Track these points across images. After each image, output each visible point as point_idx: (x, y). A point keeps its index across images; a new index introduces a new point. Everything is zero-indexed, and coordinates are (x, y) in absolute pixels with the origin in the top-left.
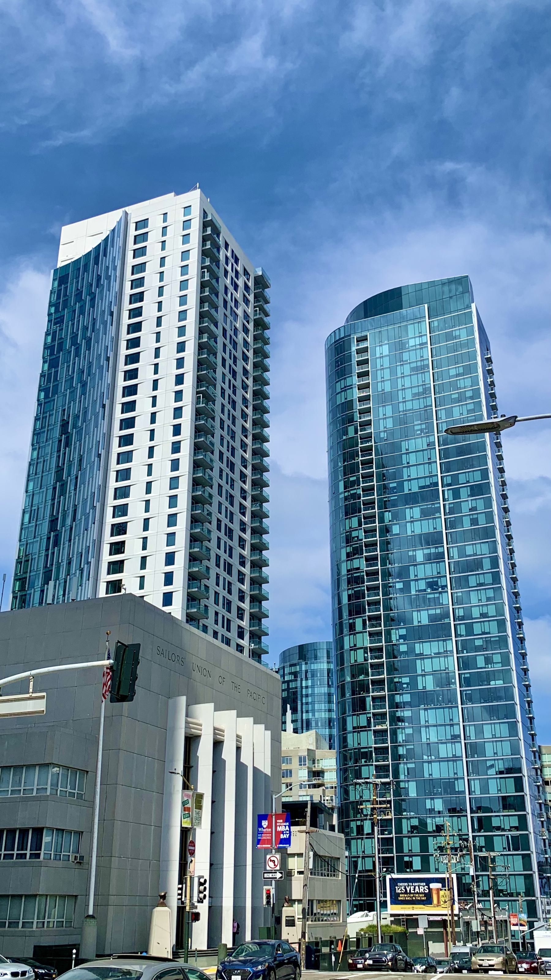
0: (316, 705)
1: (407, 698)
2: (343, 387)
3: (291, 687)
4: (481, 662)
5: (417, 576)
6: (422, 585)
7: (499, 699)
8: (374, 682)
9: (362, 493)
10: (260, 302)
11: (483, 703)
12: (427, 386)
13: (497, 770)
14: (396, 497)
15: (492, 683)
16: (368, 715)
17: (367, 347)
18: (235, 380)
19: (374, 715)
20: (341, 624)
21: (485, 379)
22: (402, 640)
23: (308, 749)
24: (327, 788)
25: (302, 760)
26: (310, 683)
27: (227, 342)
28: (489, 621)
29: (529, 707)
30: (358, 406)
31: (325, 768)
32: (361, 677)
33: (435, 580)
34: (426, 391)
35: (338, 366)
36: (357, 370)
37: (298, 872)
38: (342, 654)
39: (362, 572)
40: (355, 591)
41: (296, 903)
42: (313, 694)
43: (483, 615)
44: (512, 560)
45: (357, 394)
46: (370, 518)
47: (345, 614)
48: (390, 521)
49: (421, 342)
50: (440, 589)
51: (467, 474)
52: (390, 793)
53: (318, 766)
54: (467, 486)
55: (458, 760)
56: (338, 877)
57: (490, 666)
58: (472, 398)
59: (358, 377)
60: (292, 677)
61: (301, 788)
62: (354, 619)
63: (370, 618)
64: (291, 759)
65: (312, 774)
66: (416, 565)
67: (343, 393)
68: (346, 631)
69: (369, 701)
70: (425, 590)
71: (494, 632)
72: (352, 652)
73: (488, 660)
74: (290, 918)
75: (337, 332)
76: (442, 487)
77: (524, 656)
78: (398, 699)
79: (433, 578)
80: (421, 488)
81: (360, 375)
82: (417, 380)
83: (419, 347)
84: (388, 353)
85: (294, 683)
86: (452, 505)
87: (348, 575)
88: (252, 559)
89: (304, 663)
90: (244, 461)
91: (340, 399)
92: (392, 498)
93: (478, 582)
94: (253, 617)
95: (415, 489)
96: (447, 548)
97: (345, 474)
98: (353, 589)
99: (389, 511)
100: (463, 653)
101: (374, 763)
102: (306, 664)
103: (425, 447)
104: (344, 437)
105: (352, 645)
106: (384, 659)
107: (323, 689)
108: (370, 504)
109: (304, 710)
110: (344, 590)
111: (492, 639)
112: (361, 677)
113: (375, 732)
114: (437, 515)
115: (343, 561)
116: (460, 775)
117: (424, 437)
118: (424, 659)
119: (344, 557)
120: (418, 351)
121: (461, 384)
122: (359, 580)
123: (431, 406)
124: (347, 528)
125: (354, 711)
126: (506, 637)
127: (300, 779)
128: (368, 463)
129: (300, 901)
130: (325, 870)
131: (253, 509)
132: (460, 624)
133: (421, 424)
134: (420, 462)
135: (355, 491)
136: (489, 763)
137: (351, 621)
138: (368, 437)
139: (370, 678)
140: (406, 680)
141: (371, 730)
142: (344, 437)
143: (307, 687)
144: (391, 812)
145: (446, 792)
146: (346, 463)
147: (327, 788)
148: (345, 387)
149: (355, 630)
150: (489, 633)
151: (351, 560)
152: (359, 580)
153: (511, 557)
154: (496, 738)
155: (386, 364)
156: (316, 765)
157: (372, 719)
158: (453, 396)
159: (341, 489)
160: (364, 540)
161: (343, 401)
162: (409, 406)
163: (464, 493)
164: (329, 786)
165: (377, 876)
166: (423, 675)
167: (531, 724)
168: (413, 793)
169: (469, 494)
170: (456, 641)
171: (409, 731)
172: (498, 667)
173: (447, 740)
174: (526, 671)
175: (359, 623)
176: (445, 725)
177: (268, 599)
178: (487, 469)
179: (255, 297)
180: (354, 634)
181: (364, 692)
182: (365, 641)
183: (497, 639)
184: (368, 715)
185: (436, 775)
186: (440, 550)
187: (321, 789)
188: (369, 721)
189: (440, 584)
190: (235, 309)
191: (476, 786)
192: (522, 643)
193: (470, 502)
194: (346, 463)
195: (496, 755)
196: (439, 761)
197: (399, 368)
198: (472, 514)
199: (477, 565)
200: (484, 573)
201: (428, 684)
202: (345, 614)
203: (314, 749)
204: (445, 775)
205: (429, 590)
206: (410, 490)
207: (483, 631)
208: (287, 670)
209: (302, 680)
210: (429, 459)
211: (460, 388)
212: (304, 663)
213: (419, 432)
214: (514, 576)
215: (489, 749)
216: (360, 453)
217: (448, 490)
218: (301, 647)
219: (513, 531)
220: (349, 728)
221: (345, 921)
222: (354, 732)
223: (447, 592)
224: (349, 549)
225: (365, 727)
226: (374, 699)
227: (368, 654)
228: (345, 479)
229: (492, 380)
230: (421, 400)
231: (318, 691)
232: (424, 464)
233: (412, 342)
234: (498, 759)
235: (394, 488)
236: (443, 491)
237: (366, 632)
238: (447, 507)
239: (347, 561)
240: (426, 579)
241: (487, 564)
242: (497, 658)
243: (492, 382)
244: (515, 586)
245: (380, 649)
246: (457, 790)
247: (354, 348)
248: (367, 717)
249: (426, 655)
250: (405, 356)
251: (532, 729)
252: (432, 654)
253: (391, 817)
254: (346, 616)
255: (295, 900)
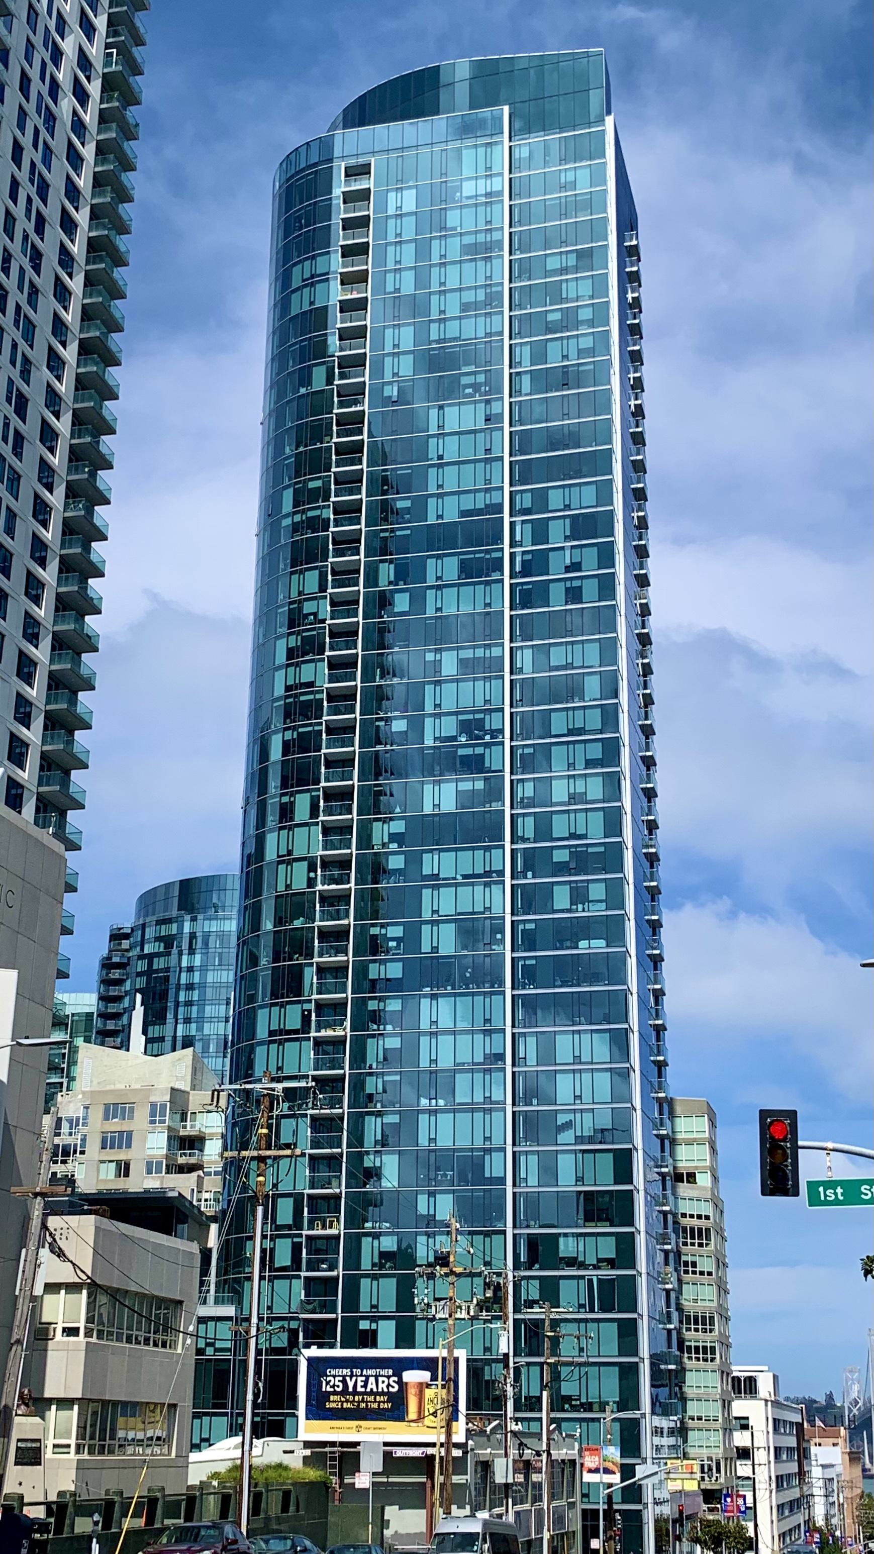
0: (208, 1008)
1: (394, 970)
2: (307, 275)
3: (155, 967)
4: (562, 898)
5: (439, 706)
6: (449, 727)
7: (595, 979)
8: (324, 935)
9: (332, 517)
10: (119, 35)
11: (561, 986)
12: (494, 289)
13: (579, 1134)
14: (409, 532)
15: (583, 944)
16: (306, 1006)
17: (369, 189)
18: (44, 201)
19: (319, 1006)
20: (262, 807)
21: (624, 372)
22: (396, 845)
23: (172, 1089)
24: (209, 1174)
25: (155, 1110)
26: (198, 960)
27: (31, 108)
28: (587, 810)
29: (657, 1003)
30: (338, 321)
31: (208, 1131)
32: (298, 923)
33: (477, 716)
34: (493, 299)
35: (301, 228)
36: (341, 239)
37: (64, 1330)
38: (259, 871)
39: (318, 692)
40: (298, 733)
41: (54, 1407)
42: (203, 986)
43: (573, 798)
44: (645, 688)
45: (337, 293)
46: (346, 575)
47: (274, 784)
48: (390, 583)
49: (489, 190)
50: (488, 738)
51: (567, 490)
52: (339, 1177)
53: (192, 1127)
54: (564, 517)
55: (497, 1110)
56: (175, 1349)
57: (580, 907)
58: (591, 323)
59: (343, 256)
60: (160, 947)
61: (149, 1172)
62: (292, 794)
63: (329, 795)
64: (132, 1110)
65: (176, 1144)
66: (438, 683)
67: (306, 291)
68: (272, 819)
69: (310, 976)
70: (454, 739)
71: (597, 836)
72: (282, 867)
73: (579, 895)
74: (29, 1445)
75: (303, 151)
76: (511, 516)
77: (657, 961)
78: (374, 972)
79: (474, 712)
80: (463, 513)
81: (348, 252)
82: (473, 274)
83: (483, 199)
84: (413, 208)
85: (162, 959)
86: (529, 557)
87: (287, 697)
88: (56, 628)
89: (188, 917)
90: (53, 399)
91: (299, 305)
92: (398, 533)
93: (571, 727)
94: (47, 763)
95: (451, 516)
96: (511, 648)
97: (298, 474)
98: (294, 728)
99: (391, 561)
100: (526, 877)
101: (310, 1112)
102: (193, 919)
103: (481, 425)
104: (303, 391)
105: (283, 851)
106: (352, 885)
107: (225, 973)
108: (347, 544)
109: (180, 1016)
110: (276, 732)
111: (590, 850)
112: (298, 923)
113: (318, 1043)
114: (495, 576)
115: (279, 668)
116: (496, 1142)
117: (480, 401)
118: (438, 887)
119: (281, 657)
120: (481, 209)
121: (570, 290)
122: (312, 710)
123: (501, 333)
124: (294, 594)
125: (274, 995)
126: (620, 846)
127: (149, 1152)
128: (351, 452)
129: (65, 1403)
130: (138, 1330)
131: (67, 515)
132: (524, 815)
133: (474, 373)
134: (465, 456)
135: (317, 512)
136: (562, 1119)
137: (285, 799)
138: (354, 394)
139: (317, 923)
140: (396, 931)
141: (309, 1039)
142: (303, 391)
143: (190, 969)
144: (338, 1221)
145: (463, 1180)
146: (301, 449)
147: (209, 1174)
148: (312, 276)
149: (292, 819)
150: (585, 837)
151: (297, 665)
152: (312, 710)
153: (645, 682)
154: (580, 1063)
155: (409, 233)
156: (188, 1123)
157: (313, 1015)
158: (551, 317)
159: (287, 504)
160: (328, 622)
161: (306, 307)
162: (452, 329)
163: (557, 535)
164: (212, 1170)
165: (253, 1332)
166: (433, 923)
167: (658, 1040)
168: (390, 1180)
169: (568, 533)
170: (512, 850)
171: (393, 1043)
172: (599, 910)
173: (474, 1064)
174: (659, 995)
175: (302, 803)
176: (473, 1032)
177: (89, 727)
178: (612, 512)
179: (110, 24)
180: (290, 828)
181: (301, 955)
182: (311, 842)
183: (602, 849)
184: (306, 1006)
185: (444, 1142)
186: (496, 652)
187: (194, 1175)
188: (306, 1019)
189: (487, 727)
190: (58, 38)
191: (531, 1167)
192: (656, 969)
193: (568, 553)
194: (301, 449)
195: (578, 1102)
196: (454, 1111)
197: (435, 244)
198: (571, 579)
199: (572, 689)
200: (584, 708)
201: (446, 941)
202: (274, 784)
203: (188, 1089)
204: (463, 1142)
205: (463, 739)
206: (440, 517)
207: (572, 831)
208: (150, 933)
209: (180, 954)
210: (488, 451)
211: (567, 300)
212: (188, 917)
213: (470, 390)
214: (649, 722)
215: (565, 1087)
216: (335, 428)
217: (523, 522)
218: (186, 885)
219: (658, 716)
220: (262, 1033)
221: (183, 1457)
222: (270, 1042)
223: (502, 743)
224: (293, 641)
225: (296, 1032)
226: (322, 970)
227: (316, 872)
228: (296, 483)
229: (638, 375)
230: (481, 320)
231: (213, 975)
232: (474, 461)
233: (468, 188)
234: (582, 1111)
235: (408, 510)
236: (512, 524)
237: (317, 823)
238: (518, 559)
239: (288, 666)
240: (456, 713)
241: (592, 686)
242: (597, 891)
243: (637, 300)
244: (647, 744)
245: (345, 864)
246: (487, 1175)
247: (338, 191)
248: (303, 1011)
249: (444, 879)
250: (453, 218)
251: (659, 1051)
252: (458, 877)
253: (337, 1232)
254: (276, 787)
255: (50, 1401)
